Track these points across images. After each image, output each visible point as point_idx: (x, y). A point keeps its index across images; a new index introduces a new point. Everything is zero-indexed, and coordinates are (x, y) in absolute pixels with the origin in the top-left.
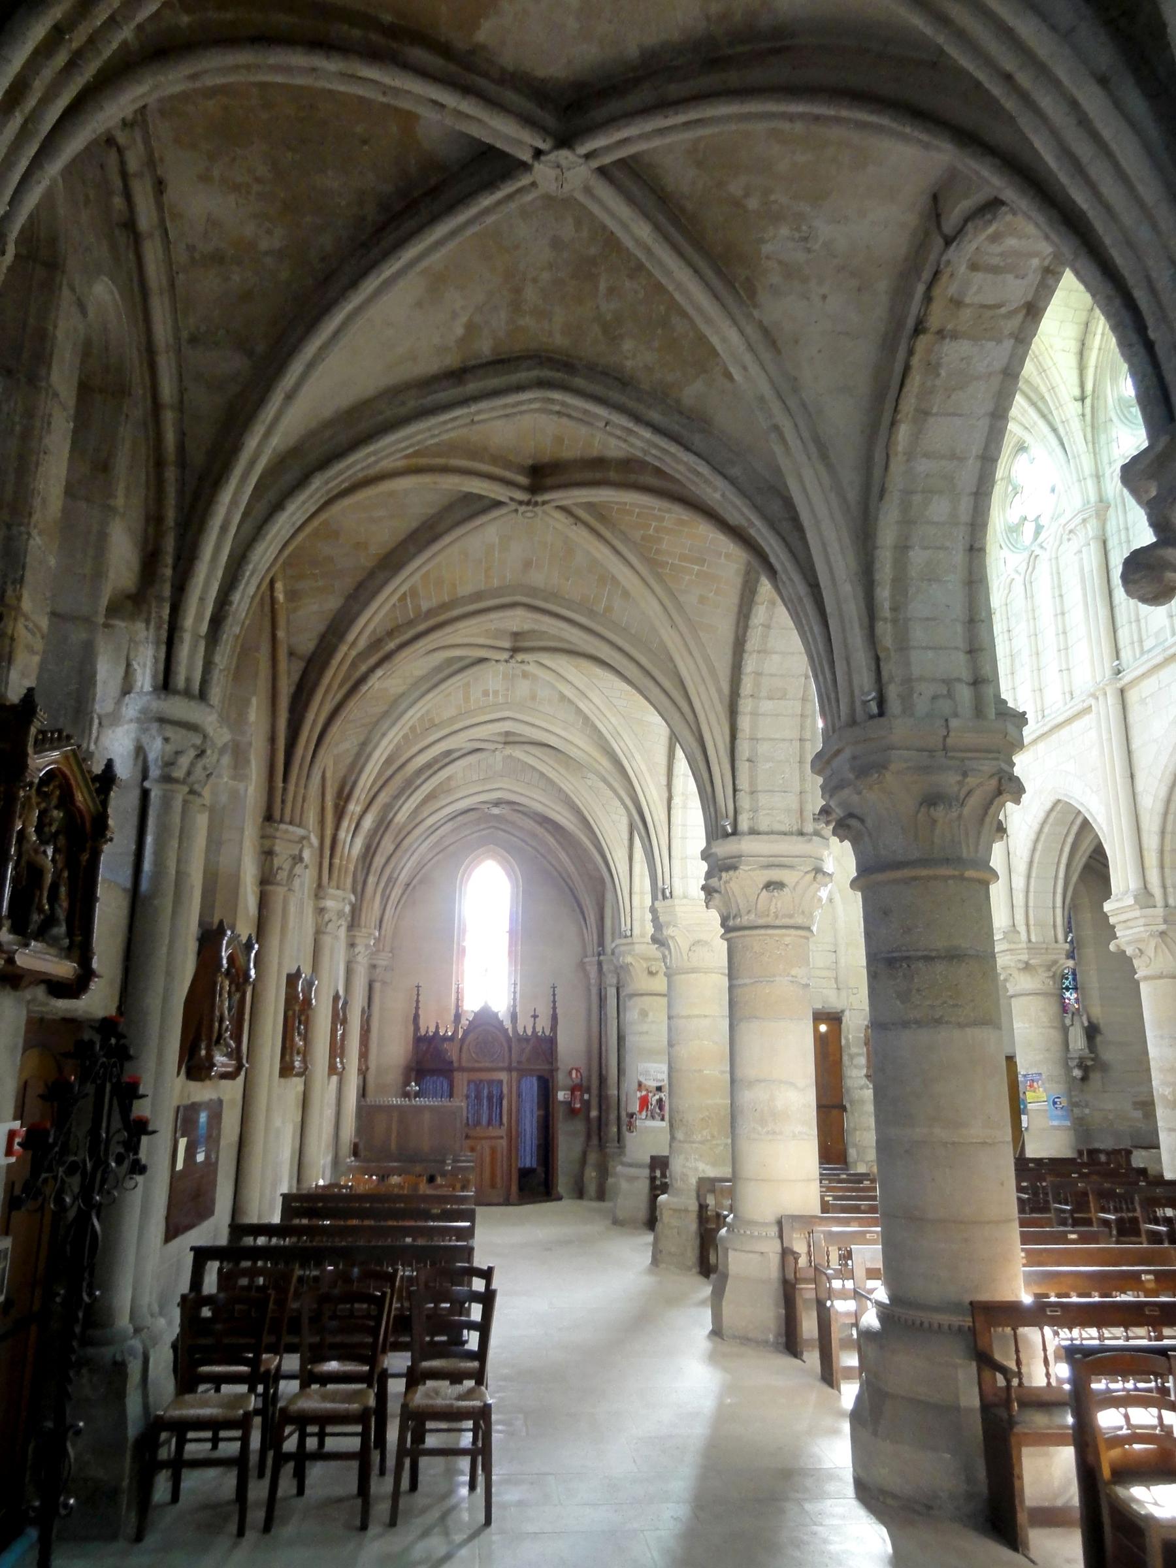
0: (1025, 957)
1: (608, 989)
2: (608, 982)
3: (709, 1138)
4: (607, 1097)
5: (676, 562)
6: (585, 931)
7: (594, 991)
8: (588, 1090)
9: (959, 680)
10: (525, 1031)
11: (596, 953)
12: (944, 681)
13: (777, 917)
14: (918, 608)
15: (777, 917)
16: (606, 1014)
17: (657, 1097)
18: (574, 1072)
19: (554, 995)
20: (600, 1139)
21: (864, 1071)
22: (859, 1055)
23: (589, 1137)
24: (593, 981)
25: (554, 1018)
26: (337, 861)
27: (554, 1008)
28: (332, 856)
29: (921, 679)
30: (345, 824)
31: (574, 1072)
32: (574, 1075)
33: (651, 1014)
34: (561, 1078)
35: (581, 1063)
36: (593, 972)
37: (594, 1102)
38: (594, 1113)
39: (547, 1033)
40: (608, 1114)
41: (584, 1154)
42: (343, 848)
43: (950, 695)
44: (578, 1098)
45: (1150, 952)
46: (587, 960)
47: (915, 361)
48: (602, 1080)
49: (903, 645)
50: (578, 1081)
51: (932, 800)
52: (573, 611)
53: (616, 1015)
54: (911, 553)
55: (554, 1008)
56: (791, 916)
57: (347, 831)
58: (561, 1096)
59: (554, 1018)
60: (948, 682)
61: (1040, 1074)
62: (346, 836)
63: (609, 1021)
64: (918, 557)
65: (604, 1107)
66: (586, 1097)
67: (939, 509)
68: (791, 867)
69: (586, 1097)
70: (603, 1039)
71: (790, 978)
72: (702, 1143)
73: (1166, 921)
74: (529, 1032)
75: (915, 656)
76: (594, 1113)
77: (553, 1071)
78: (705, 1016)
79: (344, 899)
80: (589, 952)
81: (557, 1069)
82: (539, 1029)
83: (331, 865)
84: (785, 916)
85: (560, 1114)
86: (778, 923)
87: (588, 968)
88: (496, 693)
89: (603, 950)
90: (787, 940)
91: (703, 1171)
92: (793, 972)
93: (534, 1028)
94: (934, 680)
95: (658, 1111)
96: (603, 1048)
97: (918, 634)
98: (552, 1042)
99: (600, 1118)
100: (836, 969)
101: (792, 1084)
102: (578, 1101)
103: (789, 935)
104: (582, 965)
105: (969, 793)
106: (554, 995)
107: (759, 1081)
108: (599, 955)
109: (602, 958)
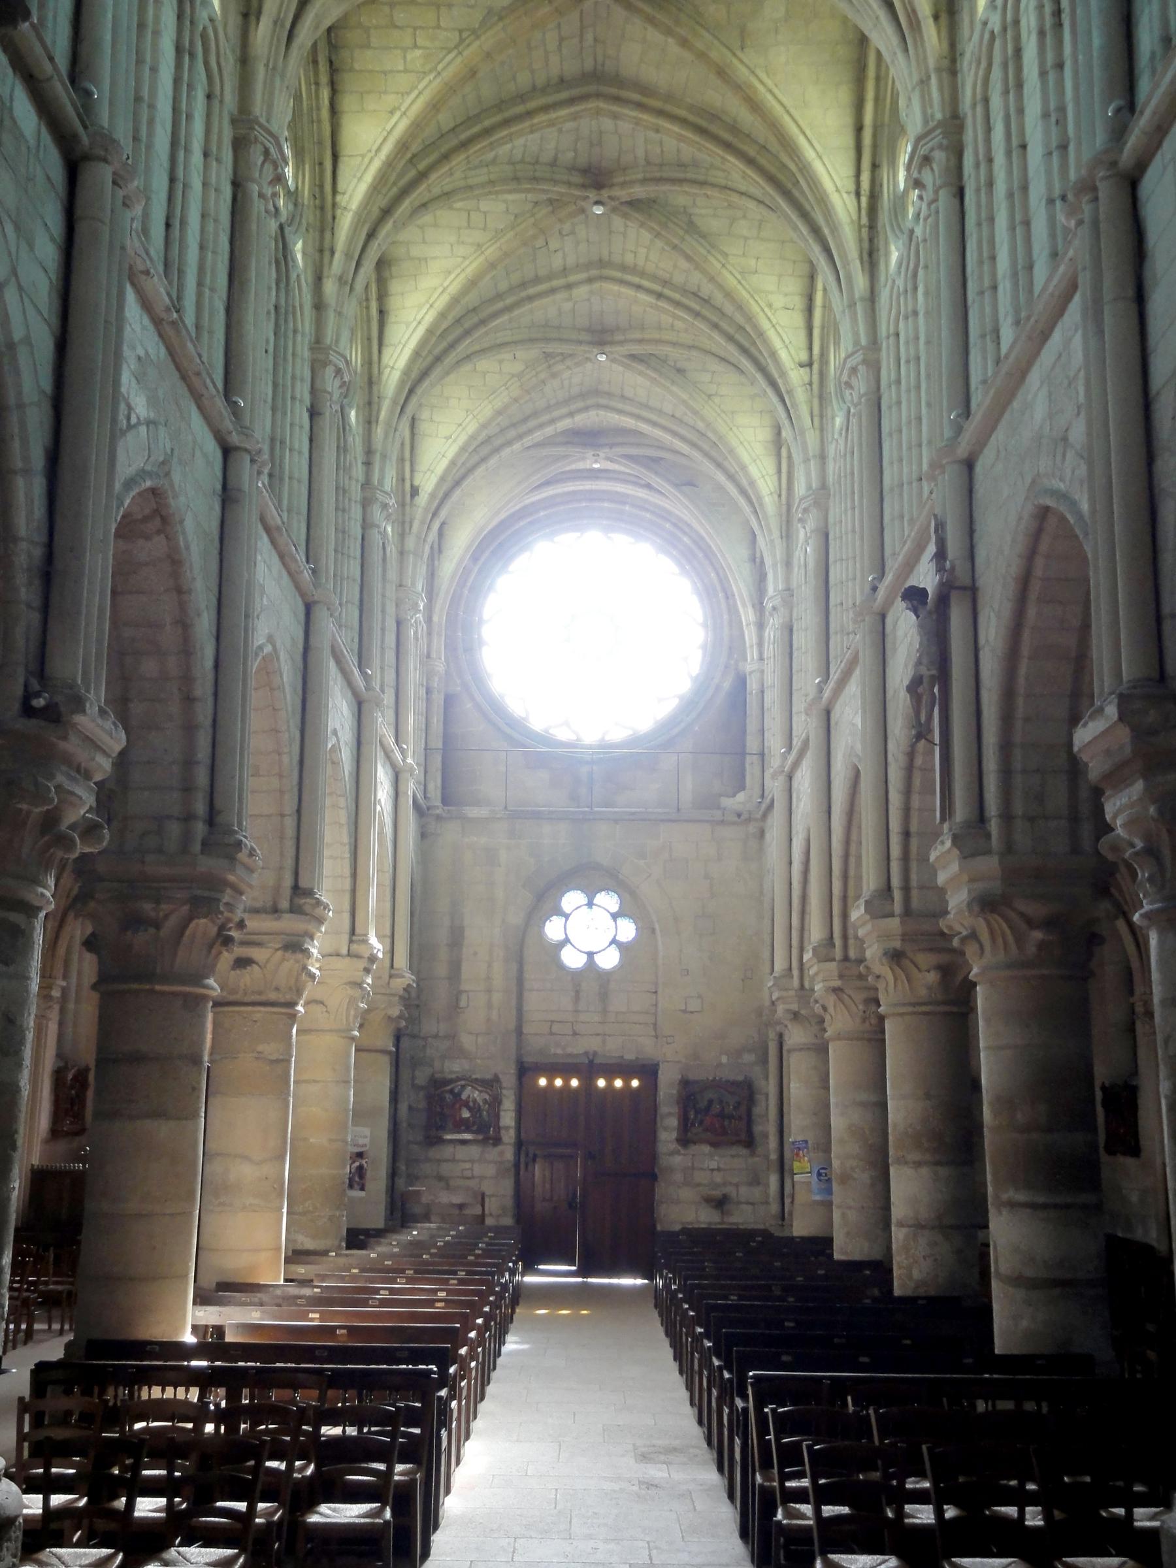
0: (794, 1007)
3: (311, 1208)
9: (169, 817)
13: (245, 994)
15: (246, 994)
17: (357, 1164)
21: (674, 1135)
22: (670, 1114)
45: (831, 1009)
51: (135, 921)
54: (131, 705)
56: (260, 993)
61: (806, 1142)
68: (258, 944)
71: (255, 1055)
72: (304, 1214)
73: (841, 977)
78: (315, 1081)
84: (253, 993)
86: (247, 999)
90: (258, 1016)
91: (302, 1244)
92: (260, 1048)
95: (357, 1179)
100: (655, 1014)
101: (246, 1158)
103: (259, 1012)
105: (166, 916)
107: (218, 1154)
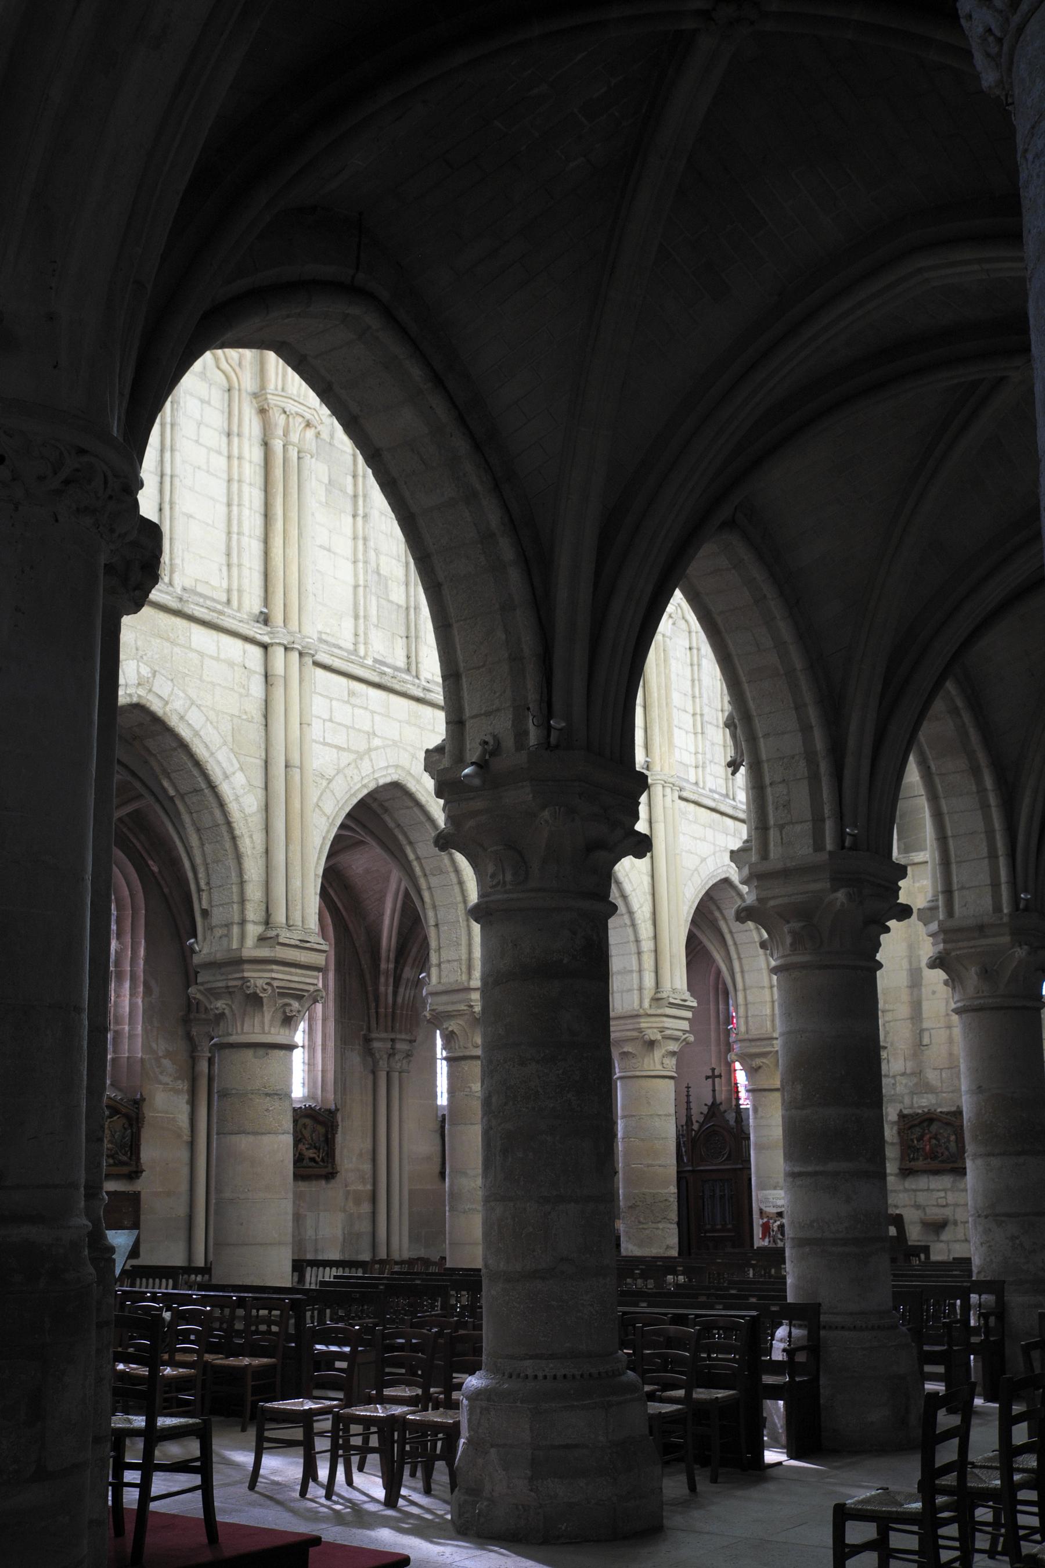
26: (382, 1010)
28: (377, 1007)
30: (382, 979)
42: (386, 999)
57: (387, 985)
62: (386, 990)
79: (393, 1040)
83: (377, 1013)
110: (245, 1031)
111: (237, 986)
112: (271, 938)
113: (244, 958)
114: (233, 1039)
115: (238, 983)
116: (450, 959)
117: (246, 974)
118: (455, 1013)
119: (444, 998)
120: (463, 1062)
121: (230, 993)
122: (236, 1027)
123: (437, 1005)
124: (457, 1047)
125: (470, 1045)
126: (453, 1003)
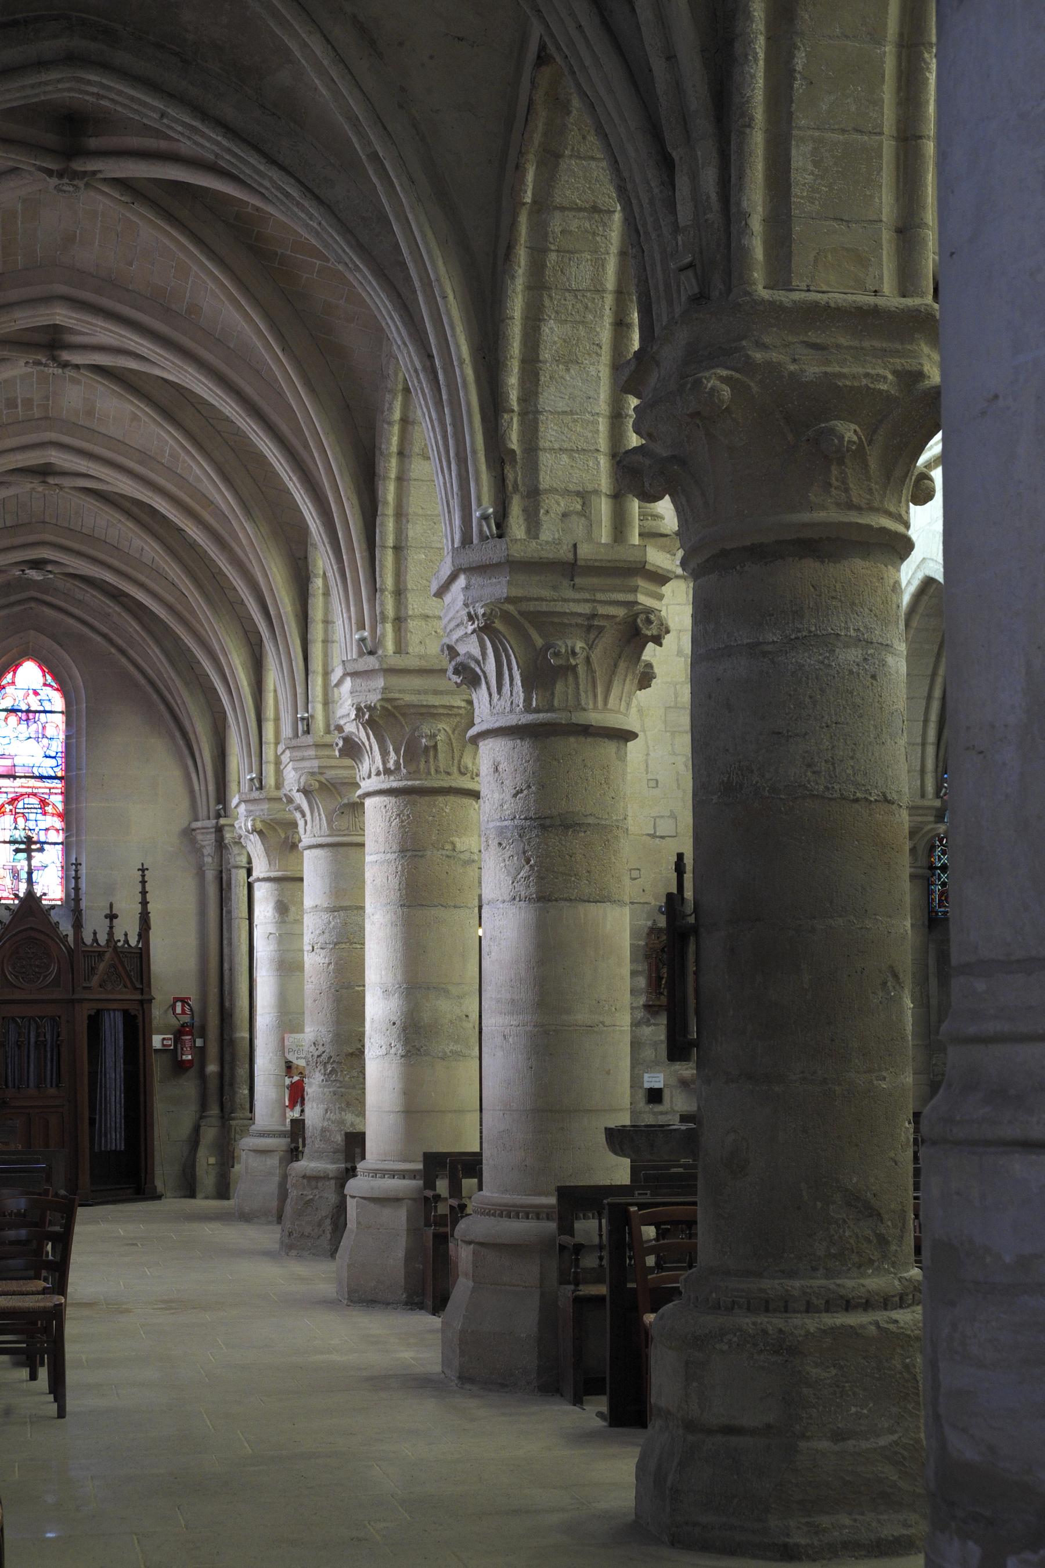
1: (233, 871)
2: (232, 861)
4: (232, 1042)
5: (289, 253)
6: (194, 776)
7: (210, 875)
8: (203, 1035)
10: (95, 940)
11: (212, 815)
12: (578, 494)
14: (550, 398)
16: (230, 912)
18: (179, 1005)
19: (143, 882)
20: (222, 1109)
23: (203, 1106)
24: (208, 860)
25: (145, 919)
27: (144, 903)
29: (553, 490)
31: (179, 1005)
32: (179, 1010)
33: (293, 909)
34: (157, 1012)
35: (190, 990)
36: (208, 842)
37: (213, 1050)
38: (212, 1068)
39: (133, 942)
40: (233, 1069)
41: (197, 1130)
43: (585, 512)
44: (188, 1044)
46: (199, 824)
47: (539, 96)
48: (226, 1015)
49: (532, 448)
50: (186, 1019)
52: (140, 309)
53: (245, 914)
55: (144, 903)
58: (157, 1041)
59: (145, 919)
60: (584, 496)
63: (235, 924)
64: (552, 331)
65: (227, 1057)
66: (199, 1042)
67: (580, 274)
69: (199, 1042)
70: (226, 951)
74: (102, 939)
75: (546, 460)
76: (212, 1068)
77: (146, 1002)
80: (202, 812)
81: (150, 1001)
82: (119, 935)
85: (158, 1068)
87: (199, 837)
88: (28, 403)
89: (224, 808)
93: (111, 934)
94: (567, 492)
96: (226, 966)
97: (550, 433)
98: (141, 956)
99: (221, 1075)
102: (186, 1049)
104: (188, 834)
106: (143, 882)
108: (218, 816)
109: (222, 821)
110: (609, 706)
111: (614, 617)
112: (666, 536)
113: (647, 567)
114: (595, 717)
115: (620, 612)
116: (430, 613)
117: (642, 598)
118: (441, 711)
119: (417, 682)
120: (441, 799)
121: (589, 628)
122: (595, 696)
123: (400, 691)
124: (433, 771)
125: (455, 770)
126: (436, 692)
